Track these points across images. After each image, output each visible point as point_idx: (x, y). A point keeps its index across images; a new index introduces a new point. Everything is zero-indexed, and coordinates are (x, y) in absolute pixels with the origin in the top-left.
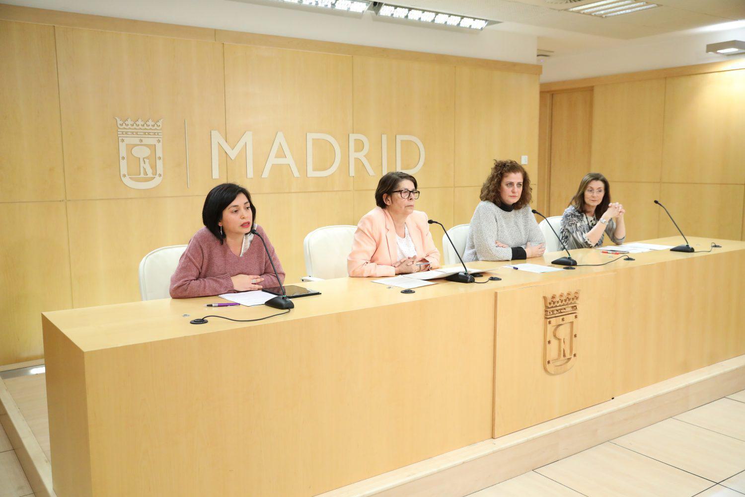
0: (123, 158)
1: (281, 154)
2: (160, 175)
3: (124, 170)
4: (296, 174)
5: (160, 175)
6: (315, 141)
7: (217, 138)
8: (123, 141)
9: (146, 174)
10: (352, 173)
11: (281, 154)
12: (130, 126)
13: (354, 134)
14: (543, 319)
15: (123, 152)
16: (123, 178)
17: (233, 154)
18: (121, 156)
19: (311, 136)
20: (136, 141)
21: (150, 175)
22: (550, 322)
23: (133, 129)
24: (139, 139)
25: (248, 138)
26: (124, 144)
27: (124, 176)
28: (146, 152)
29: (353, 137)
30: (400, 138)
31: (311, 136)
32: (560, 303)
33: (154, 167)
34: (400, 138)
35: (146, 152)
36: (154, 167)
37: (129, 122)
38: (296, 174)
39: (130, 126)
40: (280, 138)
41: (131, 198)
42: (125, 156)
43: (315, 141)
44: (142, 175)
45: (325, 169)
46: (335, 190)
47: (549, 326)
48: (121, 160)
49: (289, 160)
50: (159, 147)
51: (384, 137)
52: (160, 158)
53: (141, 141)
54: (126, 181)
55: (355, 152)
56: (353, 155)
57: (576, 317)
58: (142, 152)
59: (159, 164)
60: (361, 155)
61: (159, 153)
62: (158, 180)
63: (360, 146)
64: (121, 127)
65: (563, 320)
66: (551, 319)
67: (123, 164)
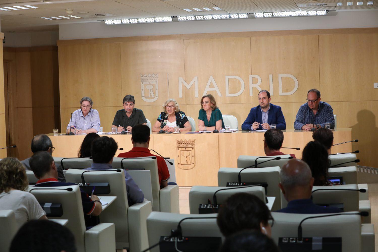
0: (143, 90)
1: (211, 86)
2: (157, 96)
3: (143, 95)
4: (220, 95)
5: (157, 96)
6: (230, 80)
7: (181, 80)
8: (142, 83)
9: (151, 96)
10: (251, 94)
11: (211, 86)
12: (145, 77)
13: (251, 75)
14: (176, 148)
15: (143, 88)
16: (142, 98)
17: (188, 87)
18: (142, 88)
19: (227, 77)
20: (148, 83)
21: (153, 96)
22: (178, 149)
23: (146, 78)
24: (149, 82)
25: (195, 80)
26: (143, 84)
27: (143, 97)
28: (152, 87)
29: (251, 77)
30: (280, 76)
31: (227, 77)
32: (183, 143)
33: (154, 93)
34: (280, 76)
35: (152, 87)
36: (154, 93)
37: (145, 76)
38: (220, 95)
39: (145, 77)
40: (211, 78)
41: (146, 106)
42: (143, 89)
43: (230, 80)
44: (150, 96)
45: (236, 93)
46: (242, 103)
47: (178, 151)
48: (142, 91)
49: (216, 89)
50: (156, 85)
51: (271, 76)
52: (157, 89)
53: (149, 83)
54: (144, 99)
55: (252, 84)
56: (251, 86)
57: (193, 149)
58: (149, 87)
59: (157, 92)
60: (256, 86)
61: (157, 88)
62: (156, 98)
63: (255, 81)
64: (143, 78)
65: (186, 149)
66: (179, 148)
67: (143, 92)
